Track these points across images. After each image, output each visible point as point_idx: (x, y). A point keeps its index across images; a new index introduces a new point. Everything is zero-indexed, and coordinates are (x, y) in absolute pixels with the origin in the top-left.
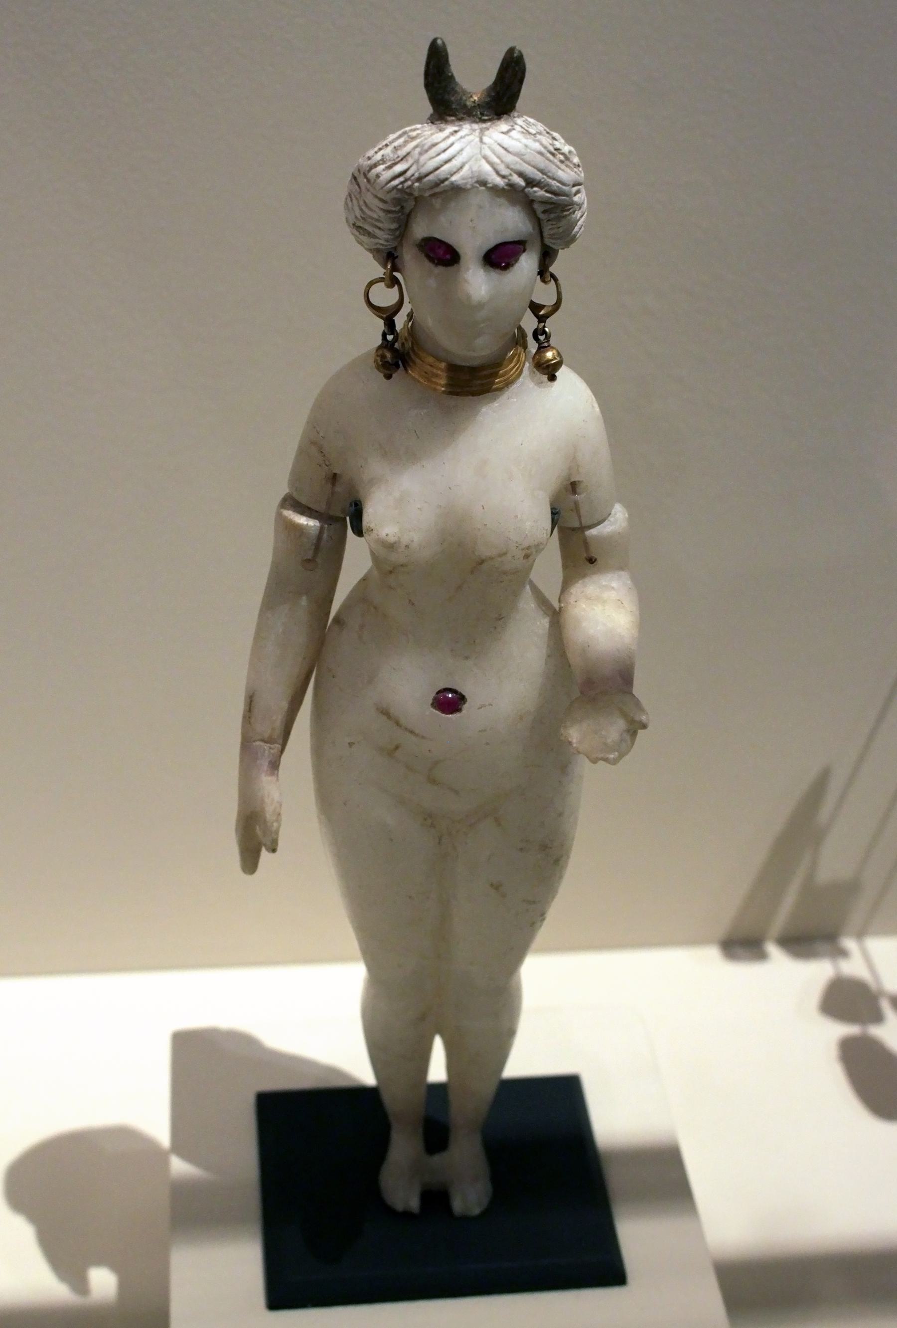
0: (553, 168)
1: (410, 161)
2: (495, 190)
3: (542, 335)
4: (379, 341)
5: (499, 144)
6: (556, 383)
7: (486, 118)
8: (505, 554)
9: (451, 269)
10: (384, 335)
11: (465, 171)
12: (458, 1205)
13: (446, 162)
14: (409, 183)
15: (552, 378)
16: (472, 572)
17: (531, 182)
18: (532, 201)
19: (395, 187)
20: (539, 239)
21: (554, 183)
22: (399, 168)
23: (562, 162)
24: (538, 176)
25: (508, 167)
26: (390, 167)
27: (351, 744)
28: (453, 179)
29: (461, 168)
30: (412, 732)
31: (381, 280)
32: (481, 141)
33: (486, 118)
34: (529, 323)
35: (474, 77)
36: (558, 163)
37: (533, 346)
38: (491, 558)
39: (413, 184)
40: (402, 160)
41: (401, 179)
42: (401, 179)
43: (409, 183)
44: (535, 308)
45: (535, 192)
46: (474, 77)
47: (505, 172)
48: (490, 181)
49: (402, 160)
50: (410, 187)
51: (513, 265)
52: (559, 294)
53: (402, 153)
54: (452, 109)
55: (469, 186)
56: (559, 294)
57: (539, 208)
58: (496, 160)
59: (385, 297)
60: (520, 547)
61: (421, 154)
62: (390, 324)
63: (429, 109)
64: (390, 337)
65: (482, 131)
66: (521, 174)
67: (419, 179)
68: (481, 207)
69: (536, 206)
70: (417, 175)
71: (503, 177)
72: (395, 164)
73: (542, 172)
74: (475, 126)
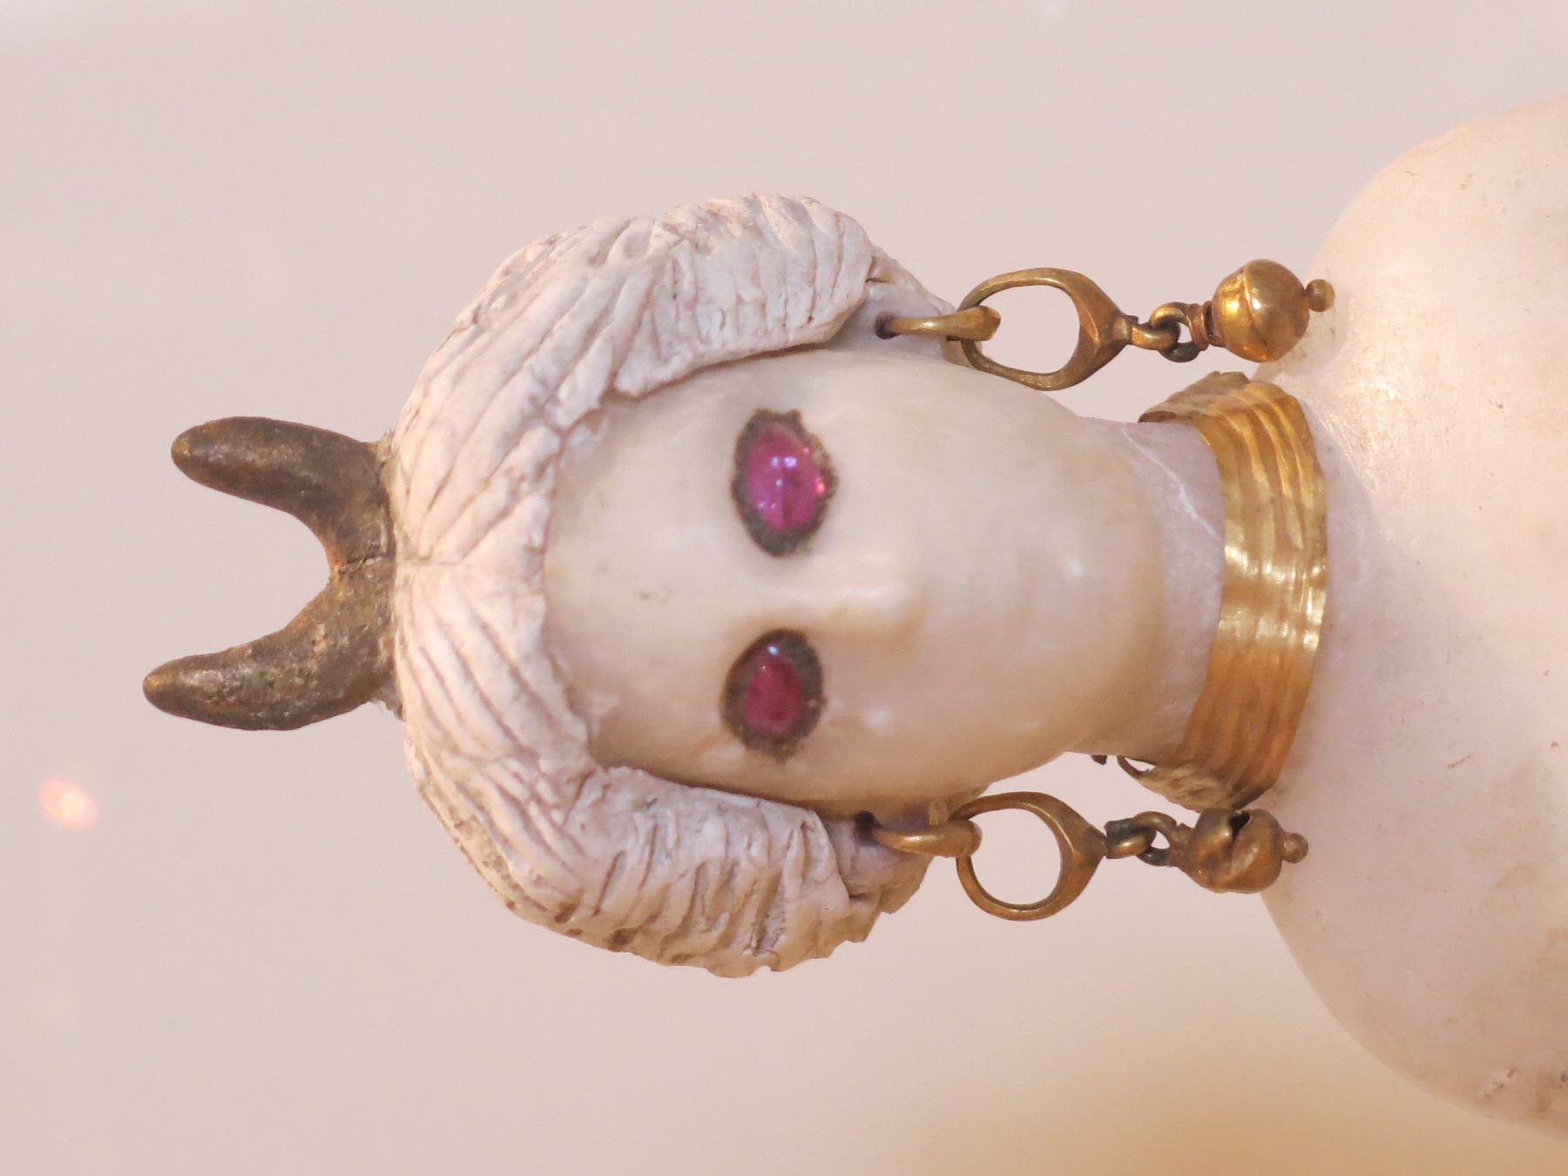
0: (517, 336)
1: (478, 783)
3: (1177, 333)
4: (1172, 875)
5: (431, 505)
6: (1339, 283)
7: (383, 540)
10: (1158, 858)
11: (497, 615)
13: (467, 673)
14: (543, 788)
15: (1317, 297)
17: (538, 410)
18: (611, 394)
19: (560, 830)
22: (506, 821)
23: (513, 298)
24: (523, 385)
25: (486, 482)
26: (506, 842)
28: (513, 654)
29: (485, 628)
31: (966, 870)
32: (425, 560)
33: (383, 540)
34: (1140, 378)
35: (272, 570)
36: (512, 312)
37: (1216, 360)
39: (543, 775)
40: (481, 808)
41: (533, 810)
42: (533, 810)
43: (543, 788)
44: (1092, 356)
45: (574, 390)
47: (500, 486)
48: (523, 541)
49: (481, 808)
50: (556, 786)
51: (826, 457)
52: (1030, 279)
53: (466, 810)
54: (355, 648)
55: (539, 605)
56: (1030, 279)
58: (465, 524)
61: (455, 751)
62: (1135, 834)
63: (370, 712)
64: (1160, 842)
65: (411, 555)
66: (511, 440)
67: (526, 754)
68: (603, 569)
69: (629, 383)
70: (515, 765)
71: (514, 495)
72: (497, 833)
73: (509, 376)
74: (403, 570)
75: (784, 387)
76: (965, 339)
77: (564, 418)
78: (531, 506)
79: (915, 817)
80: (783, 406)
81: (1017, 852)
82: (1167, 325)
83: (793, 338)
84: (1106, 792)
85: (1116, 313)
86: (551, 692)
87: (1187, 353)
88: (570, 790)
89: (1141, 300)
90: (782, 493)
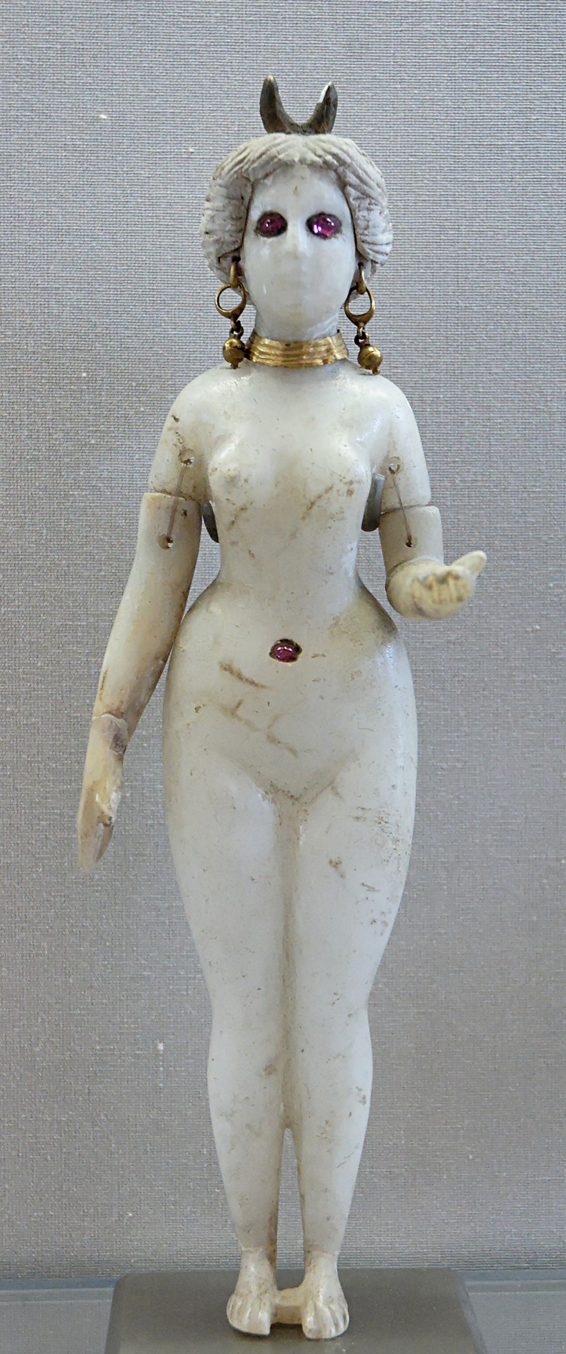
2: (312, 165)
8: (331, 488)
9: (280, 238)
12: (309, 1323)
16: (303, 518)
17: (342, 163)
20: (352, 236)
21: (360, 171)
27: (197, 709)
30: (252, 683)
34: (351, 331)
38: (320, 497)
46: (299, 107)
47: (320, 152)
57: (350, 190)
59: (232, 299)
60: (344, 480)
66: (335, 156)
71: (320, 156)
75: (347, 230)
76: (357, 287)
77: (341, 169)
78: (317, 159)
79: (239, 272)
80: (343, 228)
81: (232, 299)
82: (364, 336)
83: (359, 237)
84: (247, 320)
85: (365, 323)
86: (269, 168)
87: (357, 342)
88: (245, 175)
89: (369, 329)
90: (321, 224)
